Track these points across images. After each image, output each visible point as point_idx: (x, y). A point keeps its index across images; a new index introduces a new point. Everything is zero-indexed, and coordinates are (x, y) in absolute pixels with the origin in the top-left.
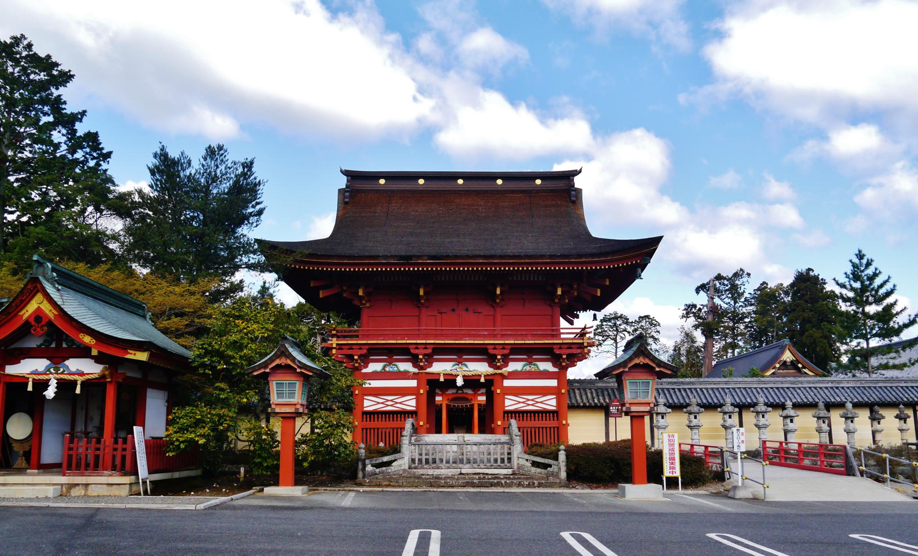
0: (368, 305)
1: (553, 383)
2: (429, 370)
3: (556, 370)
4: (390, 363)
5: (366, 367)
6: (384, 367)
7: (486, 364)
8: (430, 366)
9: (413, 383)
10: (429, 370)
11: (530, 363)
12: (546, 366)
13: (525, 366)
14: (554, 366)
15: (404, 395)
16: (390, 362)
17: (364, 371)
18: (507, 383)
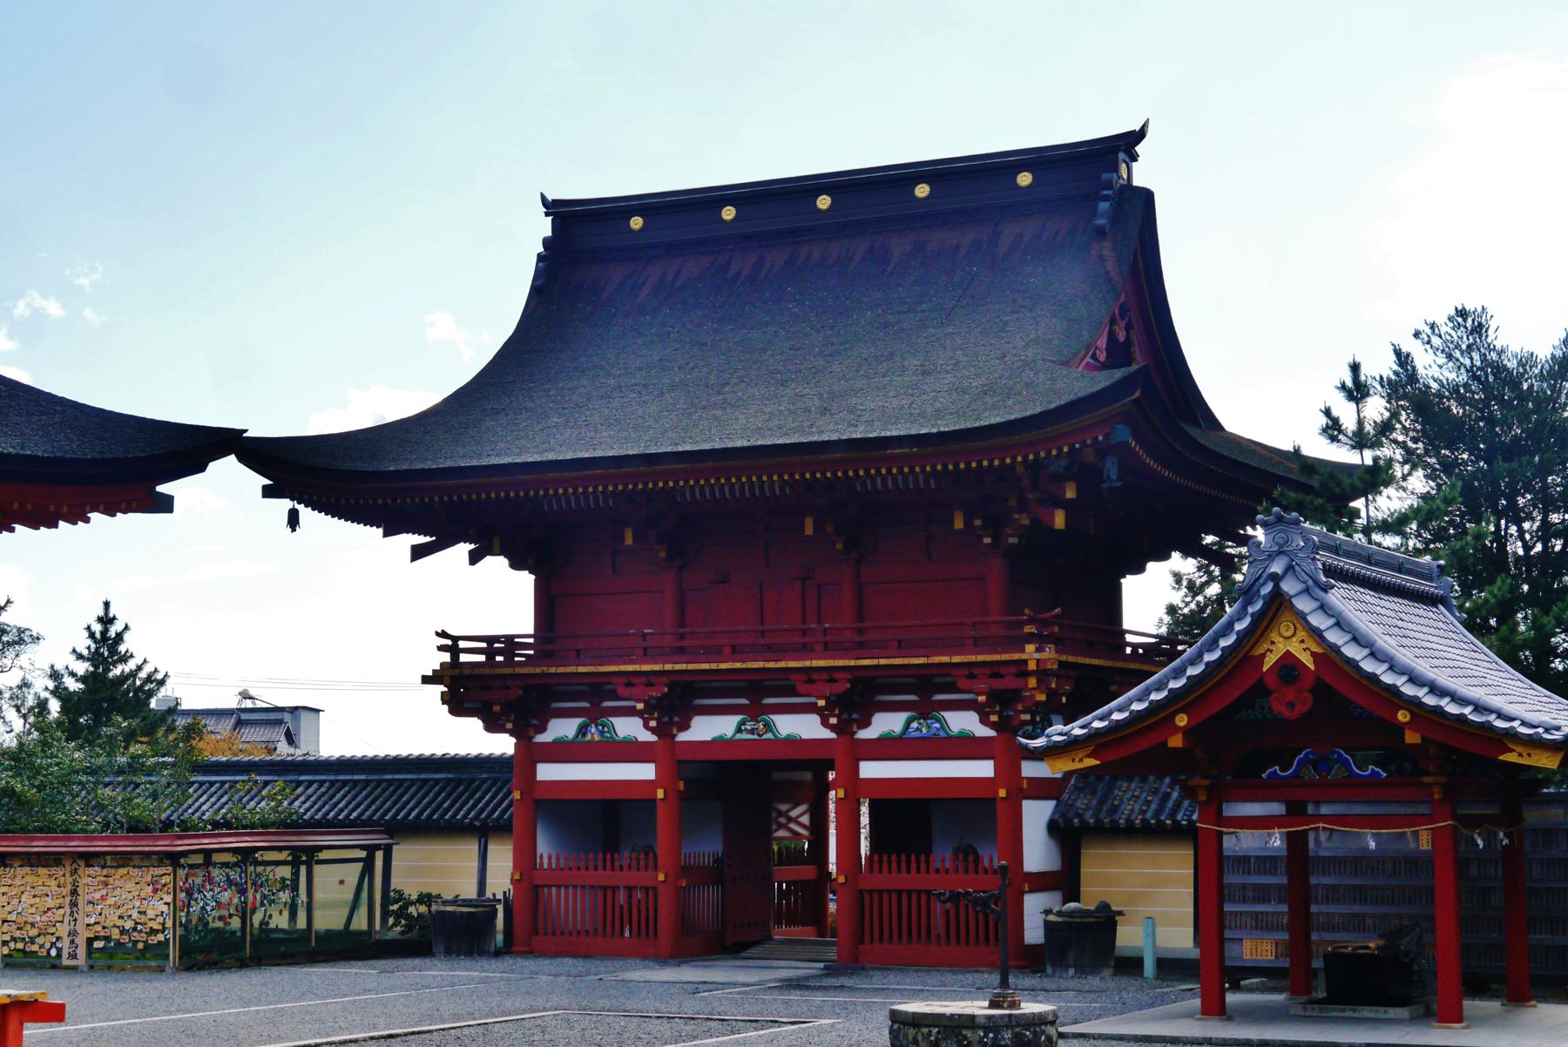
2: (683, 737)
3: (988, 732)
6: (582, 730)
8: (685, 726)
12: (964, 722)
17: (540, 738)
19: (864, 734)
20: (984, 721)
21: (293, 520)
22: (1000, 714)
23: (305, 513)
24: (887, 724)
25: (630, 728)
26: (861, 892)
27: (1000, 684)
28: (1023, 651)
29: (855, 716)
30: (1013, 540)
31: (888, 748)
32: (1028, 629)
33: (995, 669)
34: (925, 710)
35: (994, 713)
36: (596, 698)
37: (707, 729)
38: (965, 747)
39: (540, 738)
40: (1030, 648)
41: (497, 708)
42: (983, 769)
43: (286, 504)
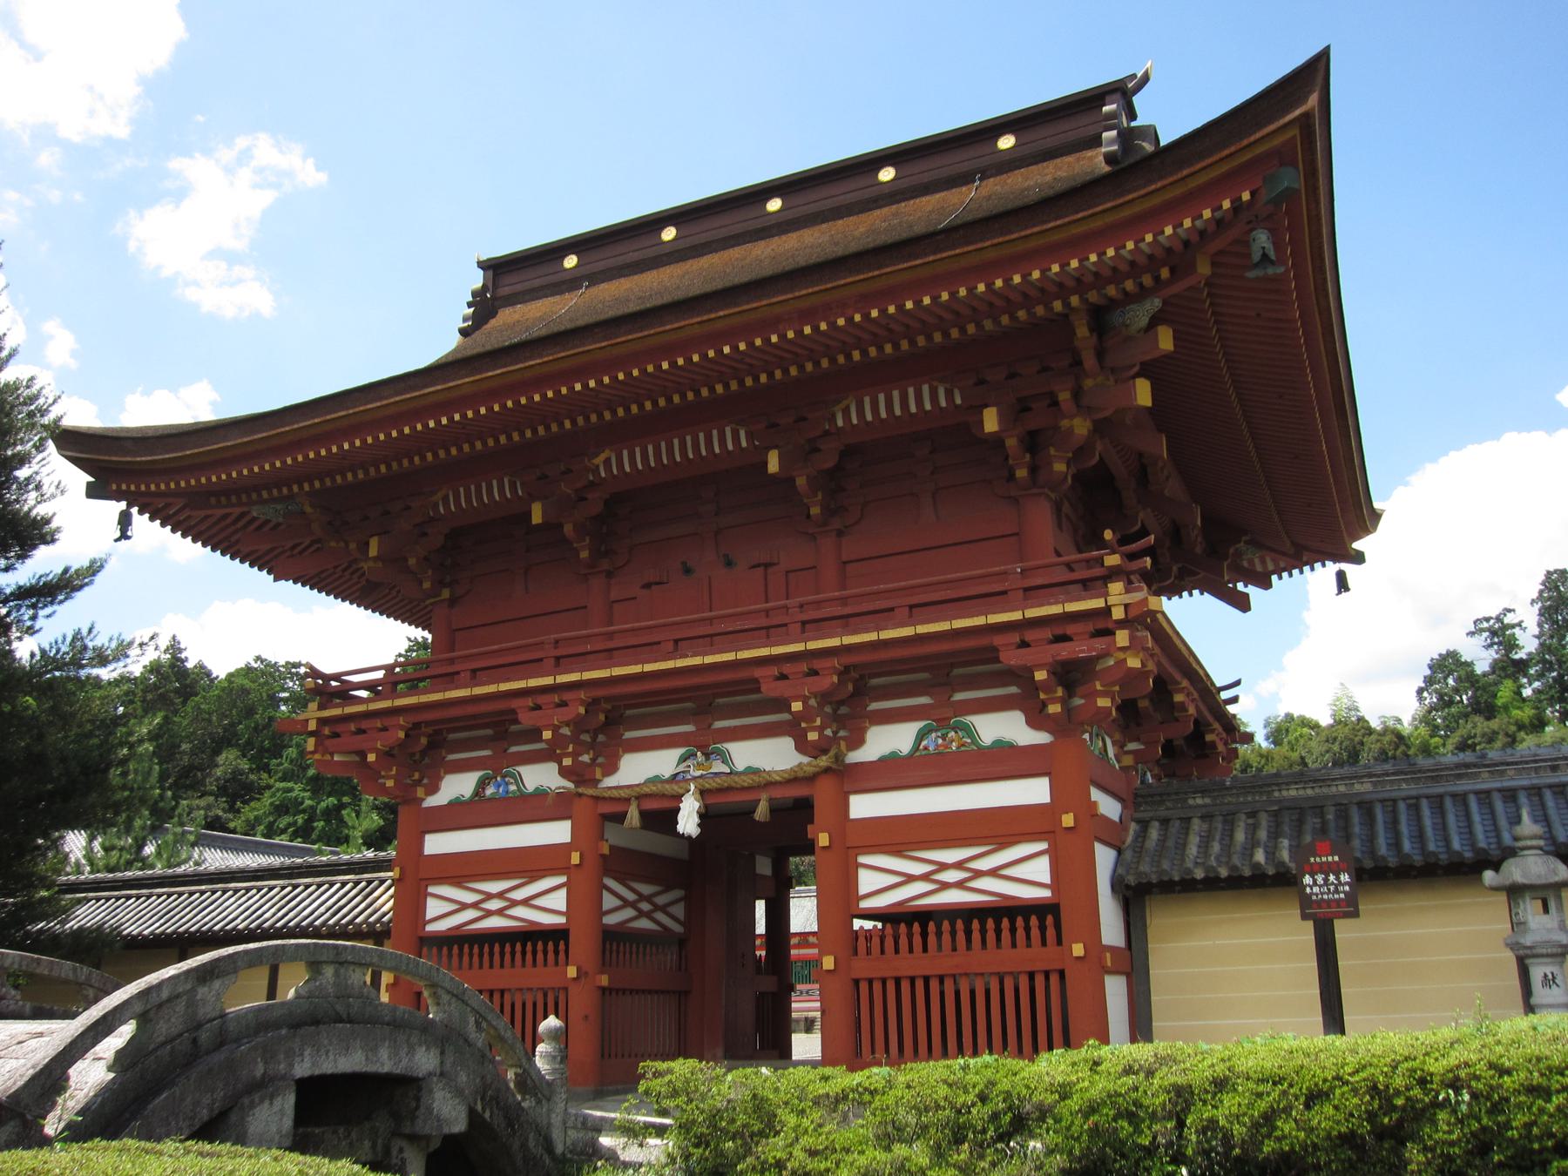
0: (446, 594)
1: (1034, 791)
4: (497, 771)
5: (433, 789)
6: (482, 784)
7: (787, 743)
8: (612, 768)
9: (557, 832)
10: (610, 781)
11: (942, 723)
12: (1003, 727)
13: (921, 736)
14: (1034, 723)
15: (533, 875)
16: (498, 767)
17: (433, 801)
18: (863, 806)
19: (855, 757)
20: (1036, 719)
21: (125, 521)
22: (1063, 702)
23: (140, 521)
24: (890, 740)
25: (541, 777)
26: (856, 982)
27: (1065, 651)
28: (1106, 595)
29: (842, 733)
30: (1060, 467)
31: (892, 773)
32: (1113, 560)
33: (1060, 629)
34: (942, 718)
35: (1054, 701)
36: (499, 733)
37: (641, 768)
38: (1004, 762)
39: (433, 801)
40: (1116, 587)
41: (371, 757)
42: (1034, 791)
43: (117, 507)
